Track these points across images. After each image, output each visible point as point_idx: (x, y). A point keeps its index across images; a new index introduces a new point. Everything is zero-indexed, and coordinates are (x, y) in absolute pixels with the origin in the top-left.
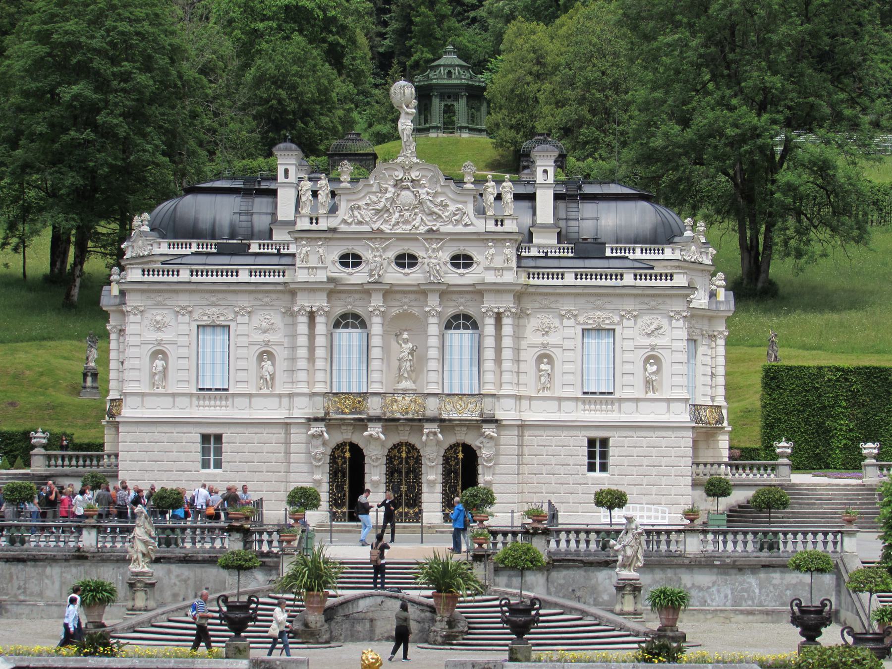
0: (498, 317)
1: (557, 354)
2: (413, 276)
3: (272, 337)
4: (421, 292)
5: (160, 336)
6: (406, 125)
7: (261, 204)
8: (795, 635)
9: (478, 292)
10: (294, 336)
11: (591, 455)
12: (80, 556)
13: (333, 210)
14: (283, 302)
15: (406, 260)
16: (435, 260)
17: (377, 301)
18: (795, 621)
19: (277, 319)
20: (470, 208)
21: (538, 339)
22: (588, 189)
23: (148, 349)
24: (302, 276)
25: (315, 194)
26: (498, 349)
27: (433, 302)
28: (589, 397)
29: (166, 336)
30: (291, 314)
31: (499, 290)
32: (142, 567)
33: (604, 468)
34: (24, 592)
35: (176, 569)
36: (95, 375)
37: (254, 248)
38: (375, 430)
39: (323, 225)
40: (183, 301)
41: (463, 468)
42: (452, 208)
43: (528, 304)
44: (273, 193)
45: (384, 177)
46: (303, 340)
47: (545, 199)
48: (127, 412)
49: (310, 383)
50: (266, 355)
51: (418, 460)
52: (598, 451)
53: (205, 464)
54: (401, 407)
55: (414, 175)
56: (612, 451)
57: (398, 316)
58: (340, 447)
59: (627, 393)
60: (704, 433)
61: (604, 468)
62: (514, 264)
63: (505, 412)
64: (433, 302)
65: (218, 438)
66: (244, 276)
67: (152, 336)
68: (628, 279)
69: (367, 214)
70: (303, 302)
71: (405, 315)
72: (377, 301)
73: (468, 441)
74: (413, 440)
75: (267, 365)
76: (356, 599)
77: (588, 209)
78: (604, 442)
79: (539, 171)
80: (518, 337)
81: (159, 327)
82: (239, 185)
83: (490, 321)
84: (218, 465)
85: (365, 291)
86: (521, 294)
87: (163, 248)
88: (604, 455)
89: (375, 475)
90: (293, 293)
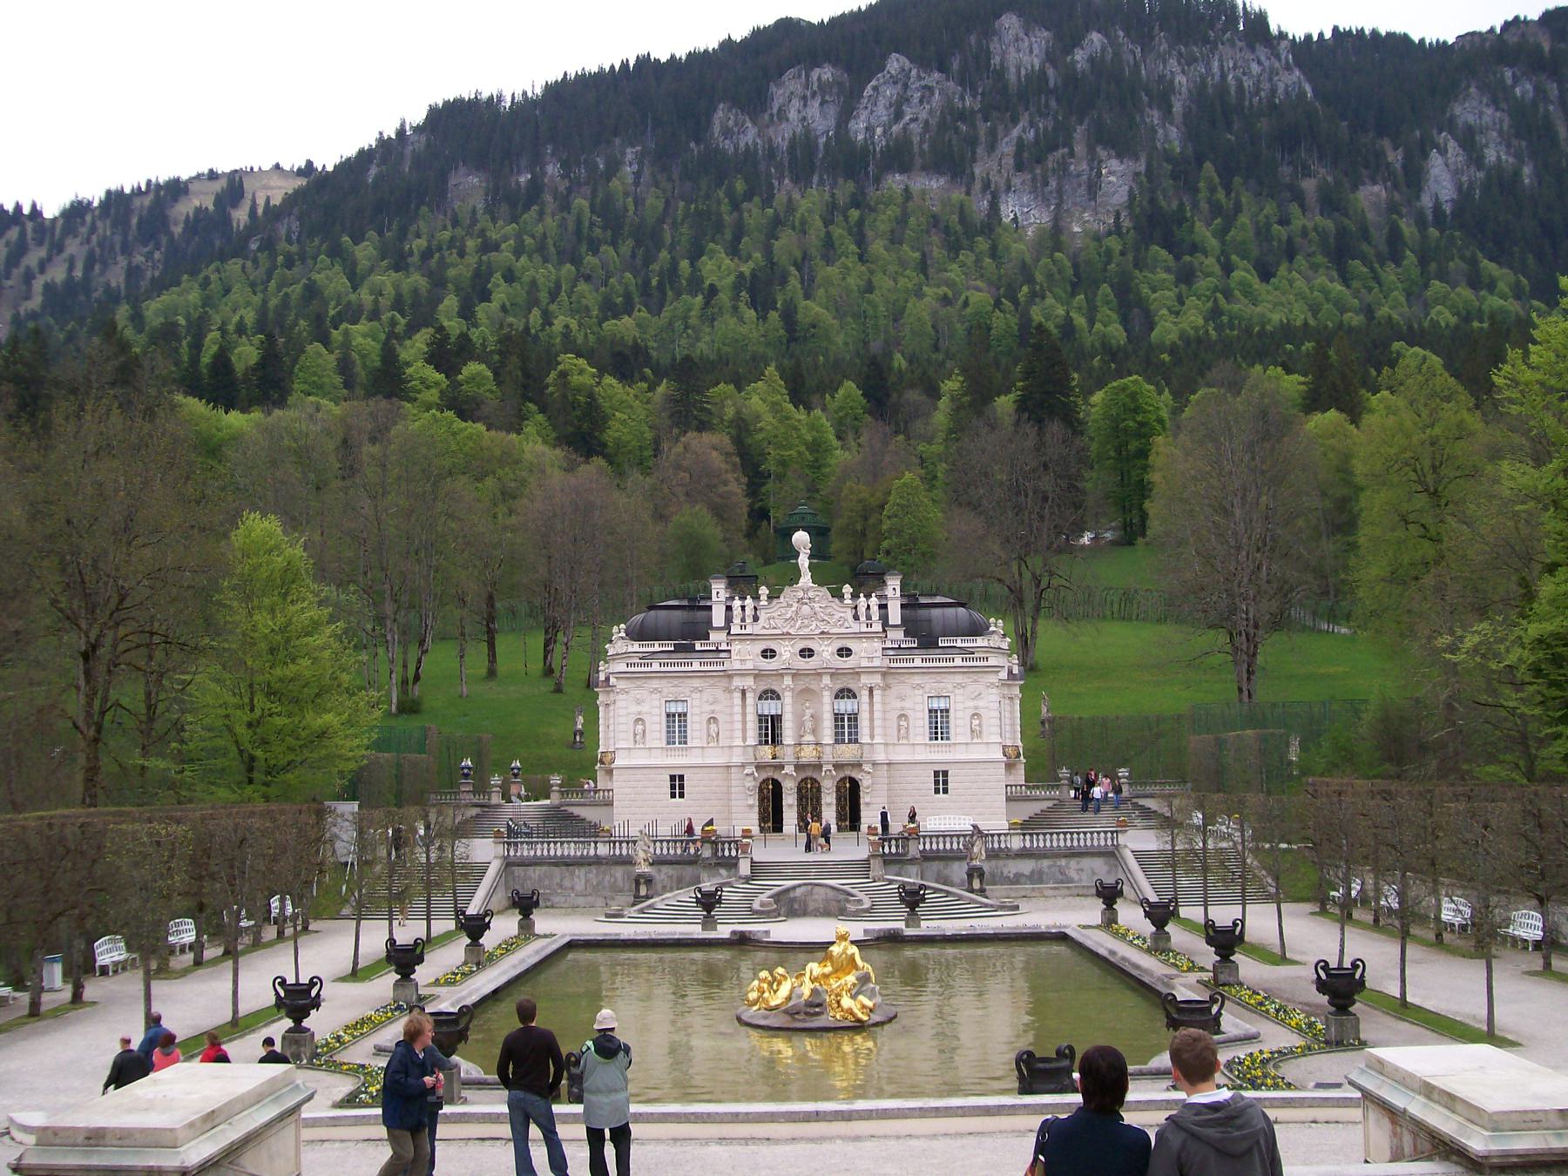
0: (871, 690)
1: (910, 713)
2: (811, 663)
3: (717, 708)
5: (639, 708)
6: (804, 561)
7: (701, 614)
8: (1099, 905)
9: (856, 673)
10: (732, 706)
11: (936, 782)
13: (756, 619)
14: (724, 683)
15: (807, 653)
16: (826, 652)
17: (788, 681)
18: (1099, 894)
19: (719, 694)
20: (850, 614)
21: (898, 704)
22: (923, 600)
23: (633, 718)
24: (737, 665)
25: (743, 608)
26: (871, 712)
27: (826, 680)
29: (644, 708)
30: (729, 691)
31: (871, 671)
32: (644, 868)
33: (945, 791)
34: (561, 886)
35: (665, 869)
36: (582, 734)
37: (698, 647)
38: (789, 769)
39: (749, 631)
40: (655, 684)
41: (850, 797)
42: (837, 616)
43: (890, 680)
46: (738, 709)
48: (618, 763)
49: (744, 739)
50: (713, 719)
51: (819, 789)
53: (673, 796)
55: (811, 594)
56: (950, 779)
57: (802, 691)
58: (765, 781)
59: (961, 739)
60: (1010, 767)
61: (945, 791)
62: (879, 653)
64: (826, 680)
65: (681, 777)
66: (696, 666)
67: (634, 708)
68: (958, 662)
69: (779, 623)
70: (738, 682)
71: (807, 691)
72: (788, 681)
73: (853, 775)
74: (815, 776)
75: (713, 726)
76: (794, 888)
77: (923, 613)
78: (945, 773)
79: (890, 588)
80: (884, 703)
81: (639, 702)
82: (685, 603)
83: (865, 693)
84: (682, 795)
85: (779, 675)
86: (886, 673)
87: (635, 647)
88: (945, 782)
89: (790, 800)
90: (730, 677)
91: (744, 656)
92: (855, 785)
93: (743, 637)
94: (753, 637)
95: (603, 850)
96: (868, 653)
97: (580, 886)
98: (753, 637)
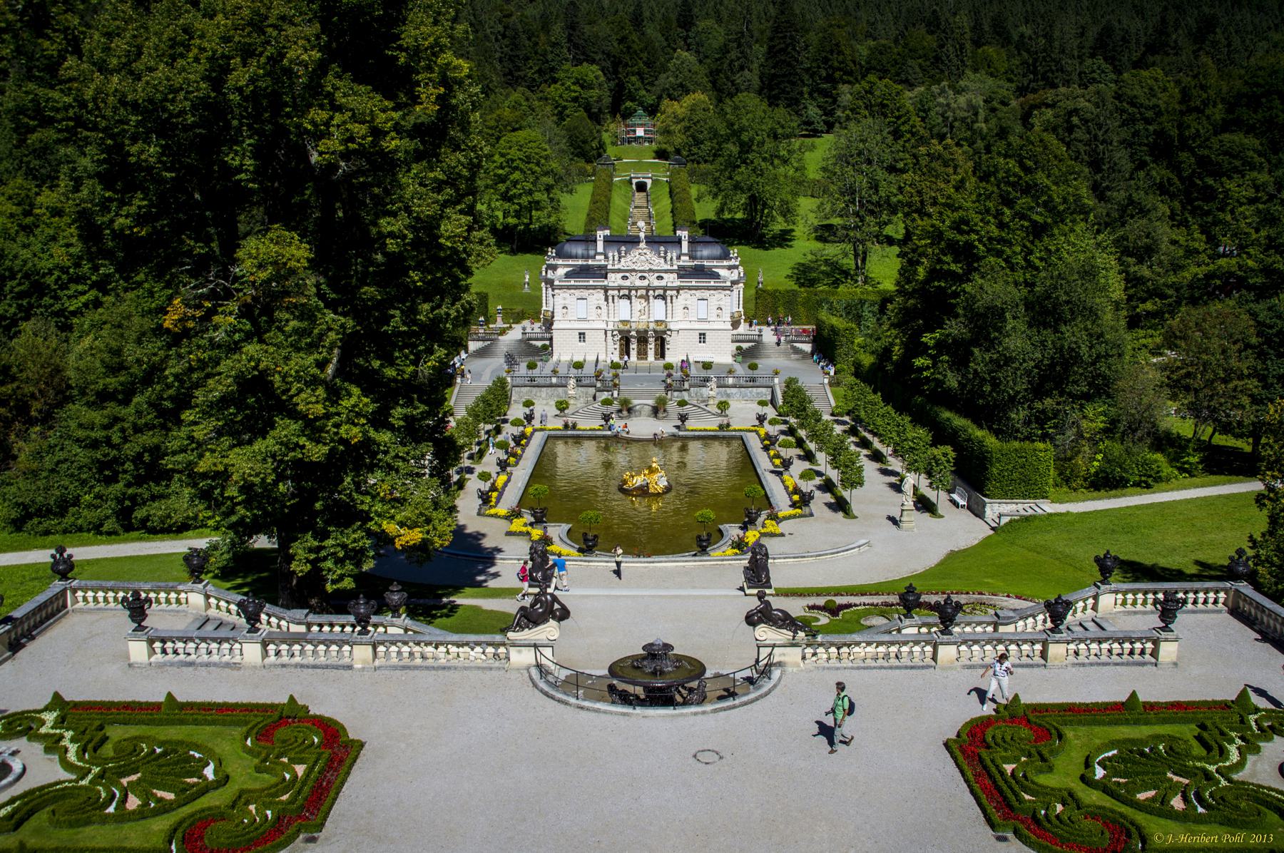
4: (648, 289)
9: (665, 289)
12: (551, 386)
28: (700, 320)
31: (672, 289)
38: (633, 333)
44: (595, 241)
45: (635, 253)
47: (685, 244)
52: (702, 337)
54: (642, 327)
63: (672, 326)
66: (591, 283)
70: (610, 292)
86: (678, 289)
87: (560, 262)
89: (634, 346)
91: (614, 280)
92: (663, 340)
93: (614, 271)
94: (619, 271)
95: (554, 380)
96: (671, 280)
97: (544, 395)
98: (619, 271)
